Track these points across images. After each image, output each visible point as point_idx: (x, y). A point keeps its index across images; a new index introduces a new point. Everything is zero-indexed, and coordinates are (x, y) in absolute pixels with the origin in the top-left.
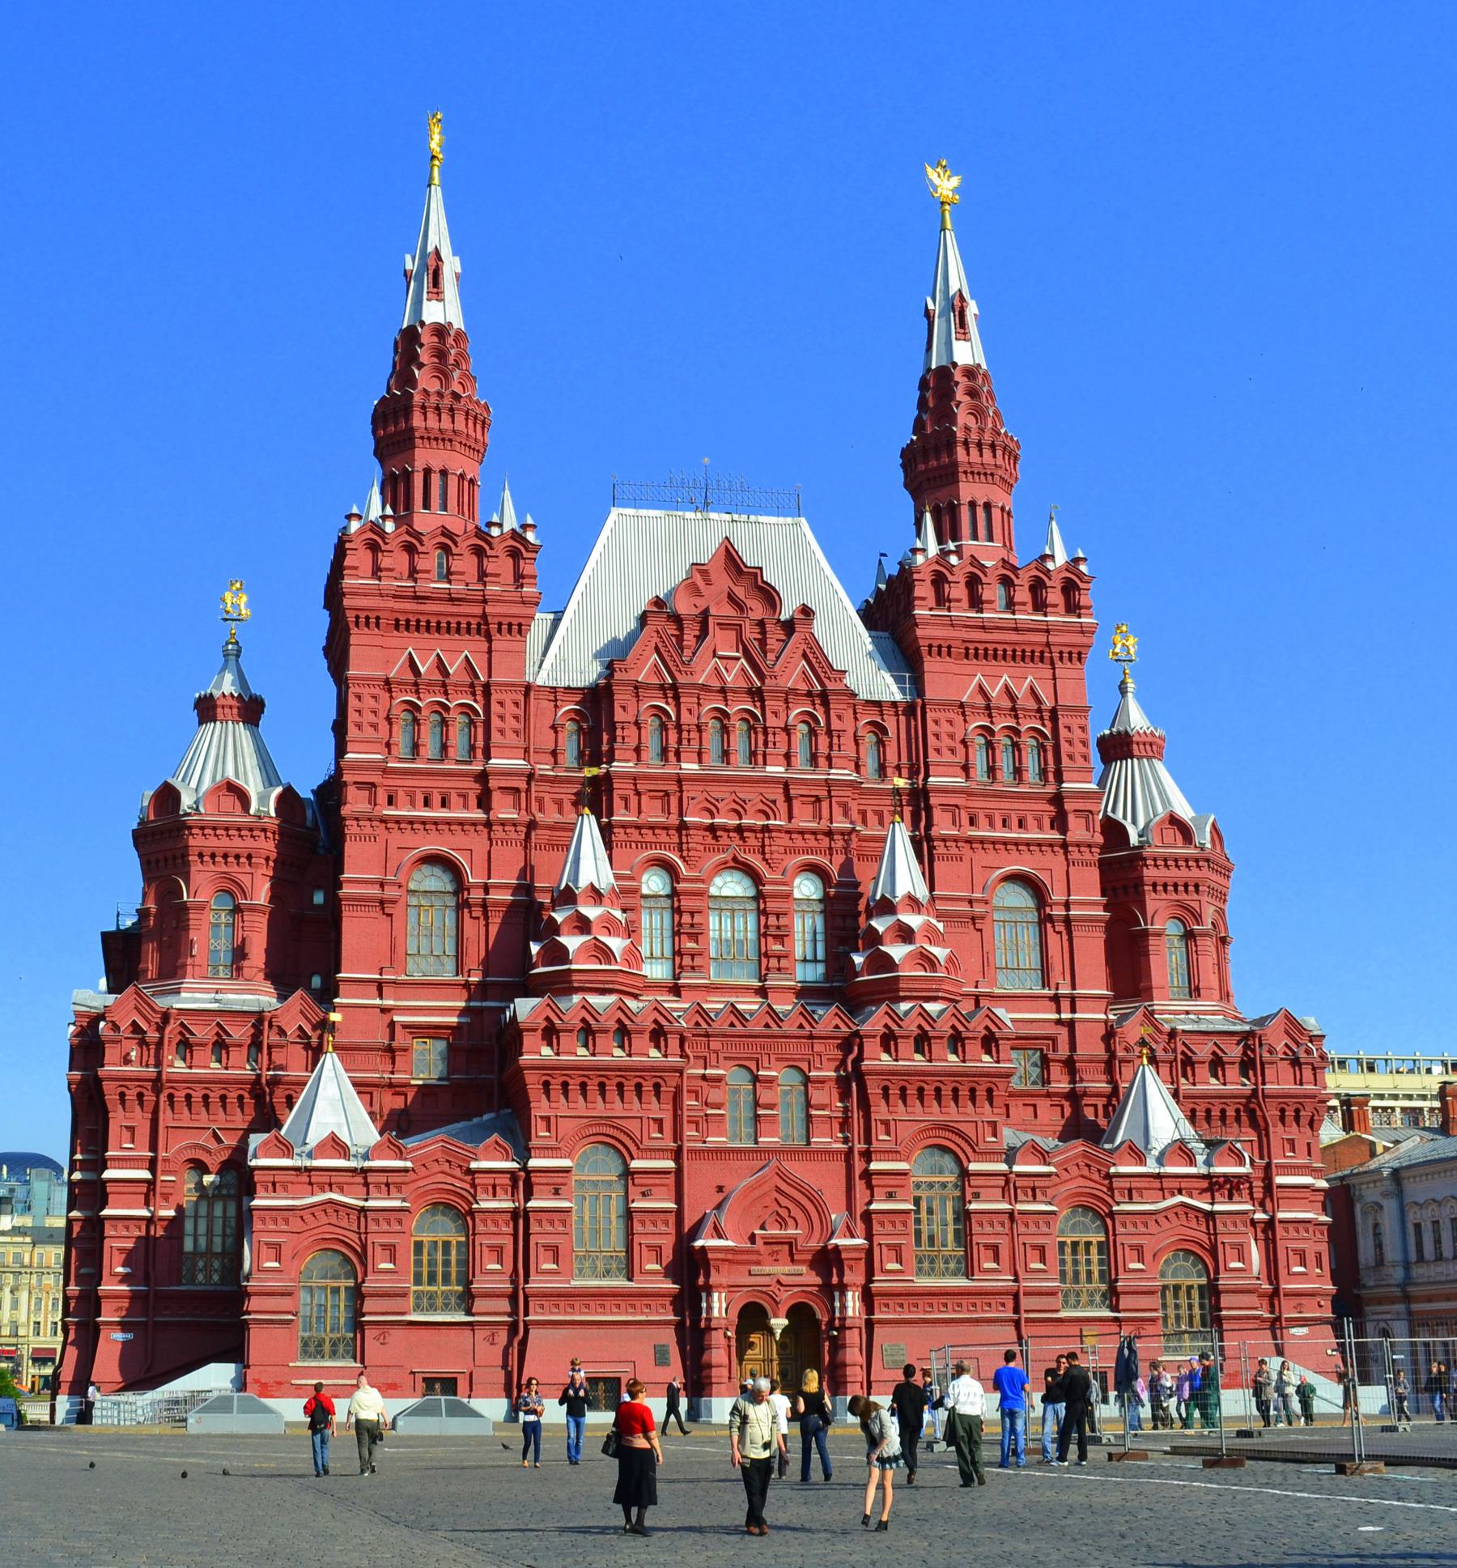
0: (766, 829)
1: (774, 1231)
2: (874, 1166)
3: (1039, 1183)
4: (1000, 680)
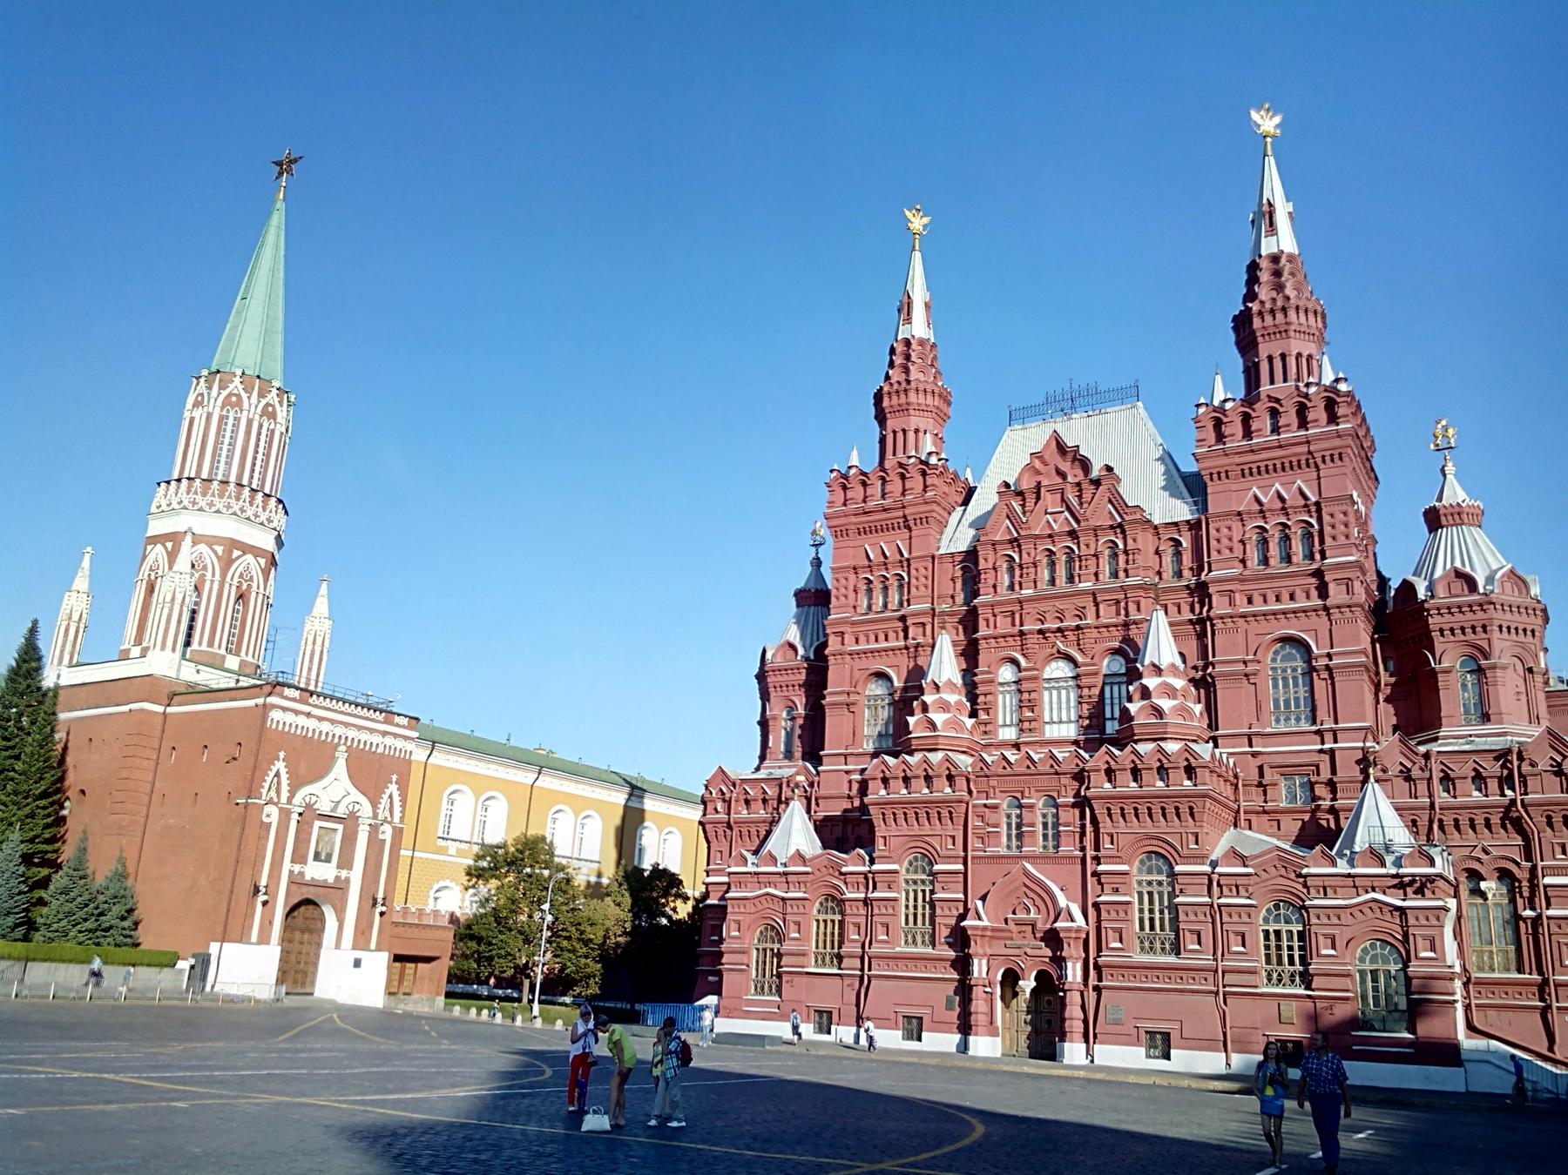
0: (1078, 628)
1: (1021, 915)
2: (1101, 868)
3: (1240, 881)
4: (1267, 491)
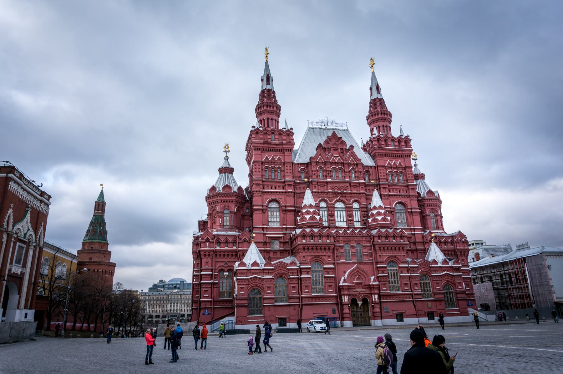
2: (378, 266)
3: (415, 269)
